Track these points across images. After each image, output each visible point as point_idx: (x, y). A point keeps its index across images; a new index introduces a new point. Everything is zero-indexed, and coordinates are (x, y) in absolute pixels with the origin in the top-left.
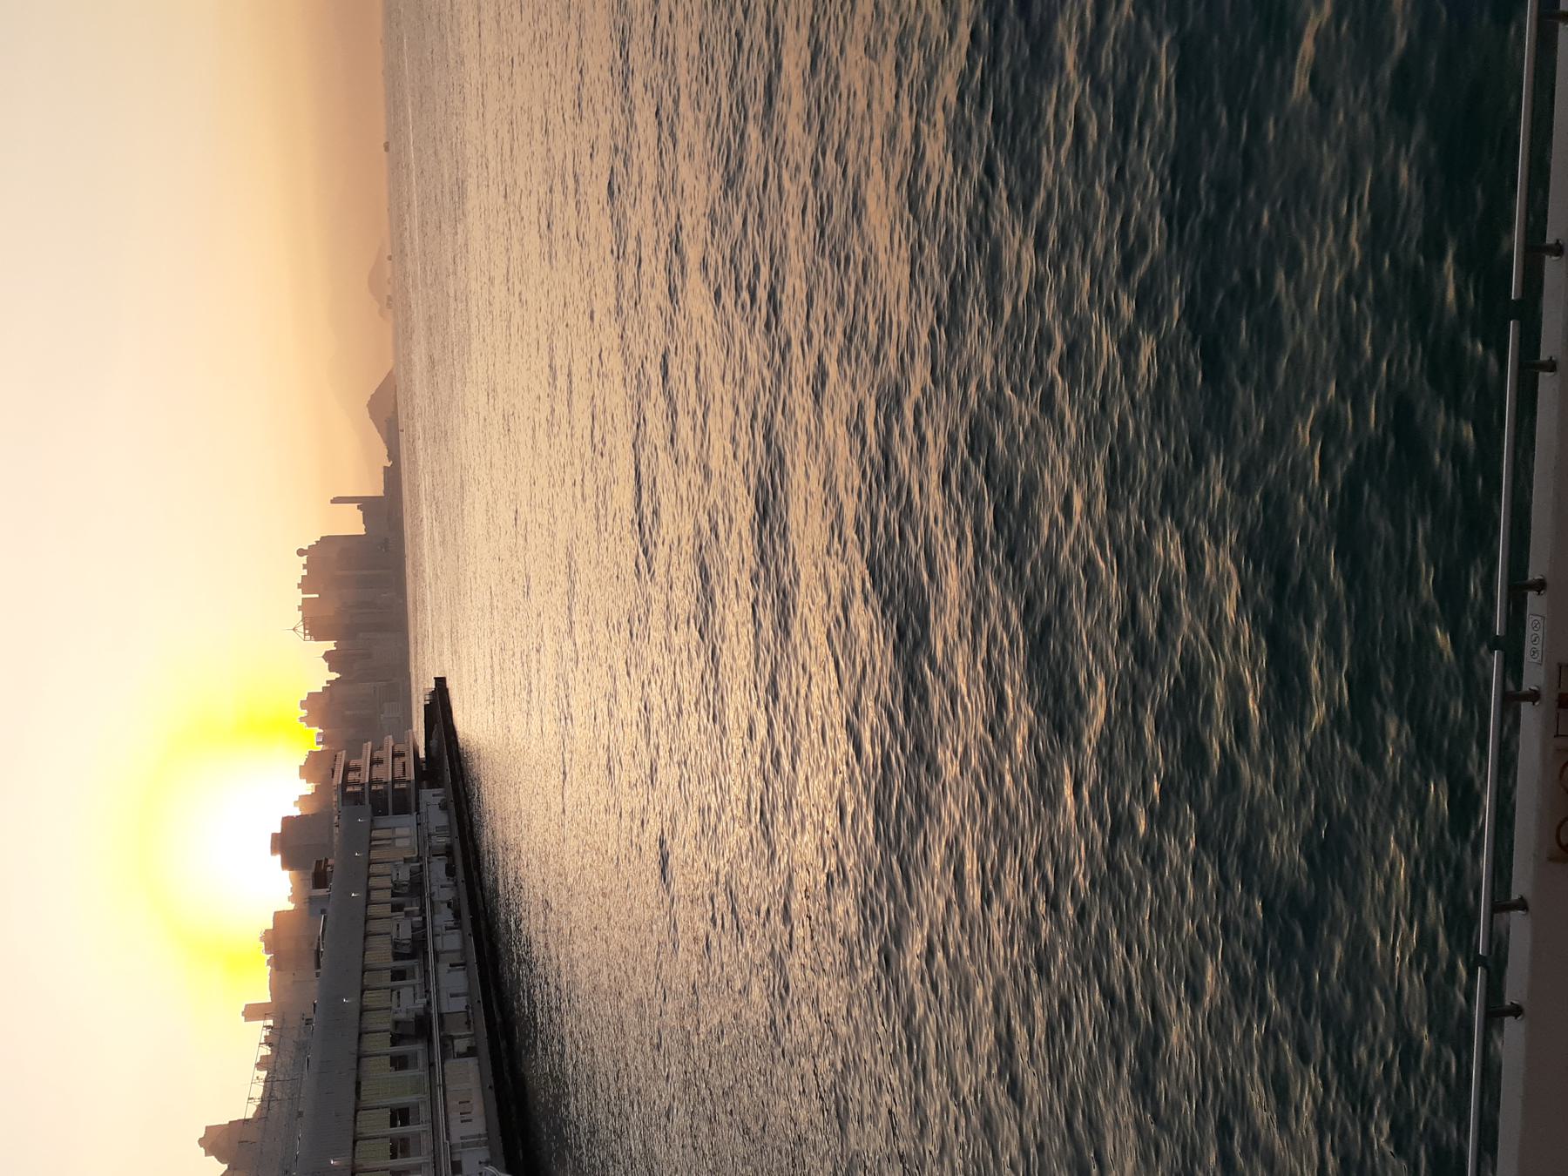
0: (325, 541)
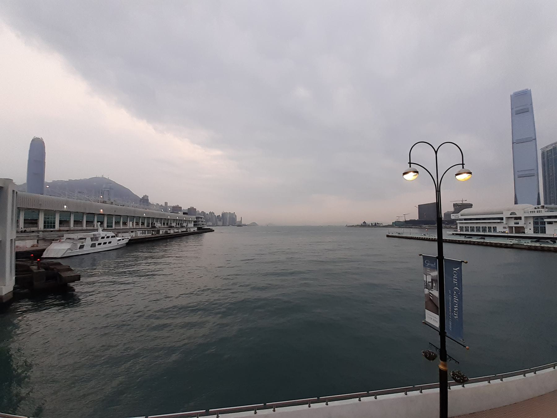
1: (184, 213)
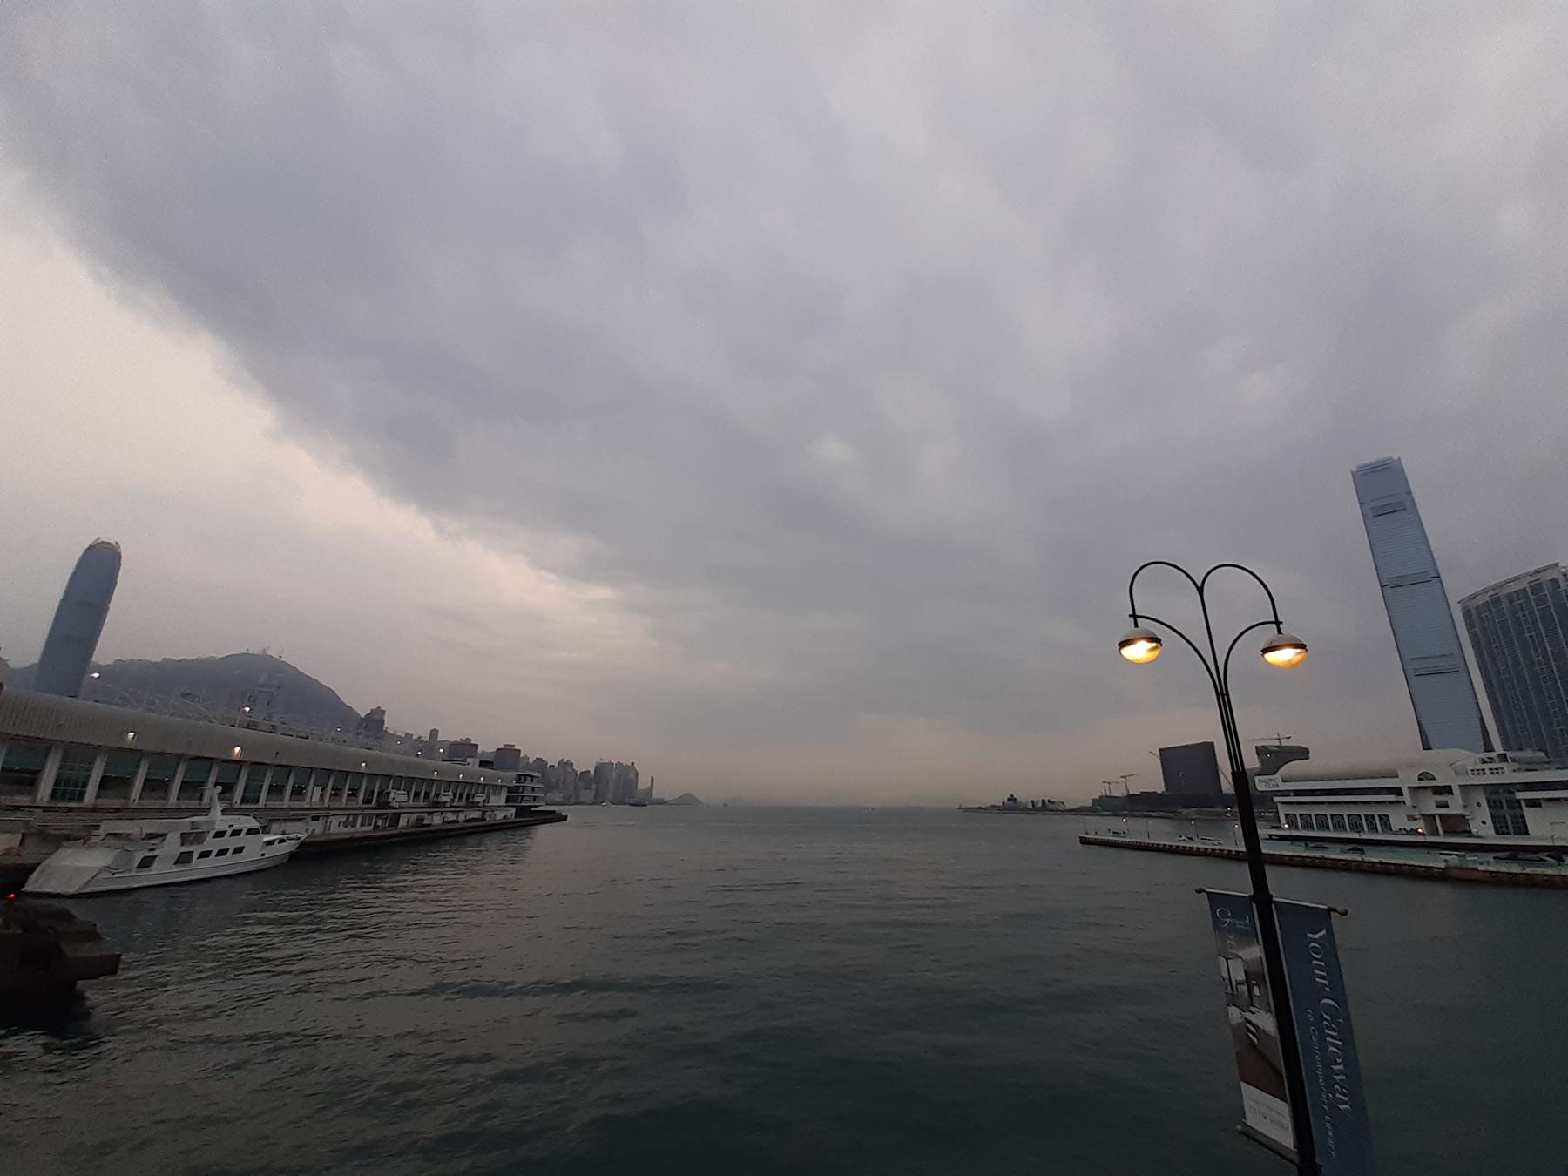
1: (483, 764)
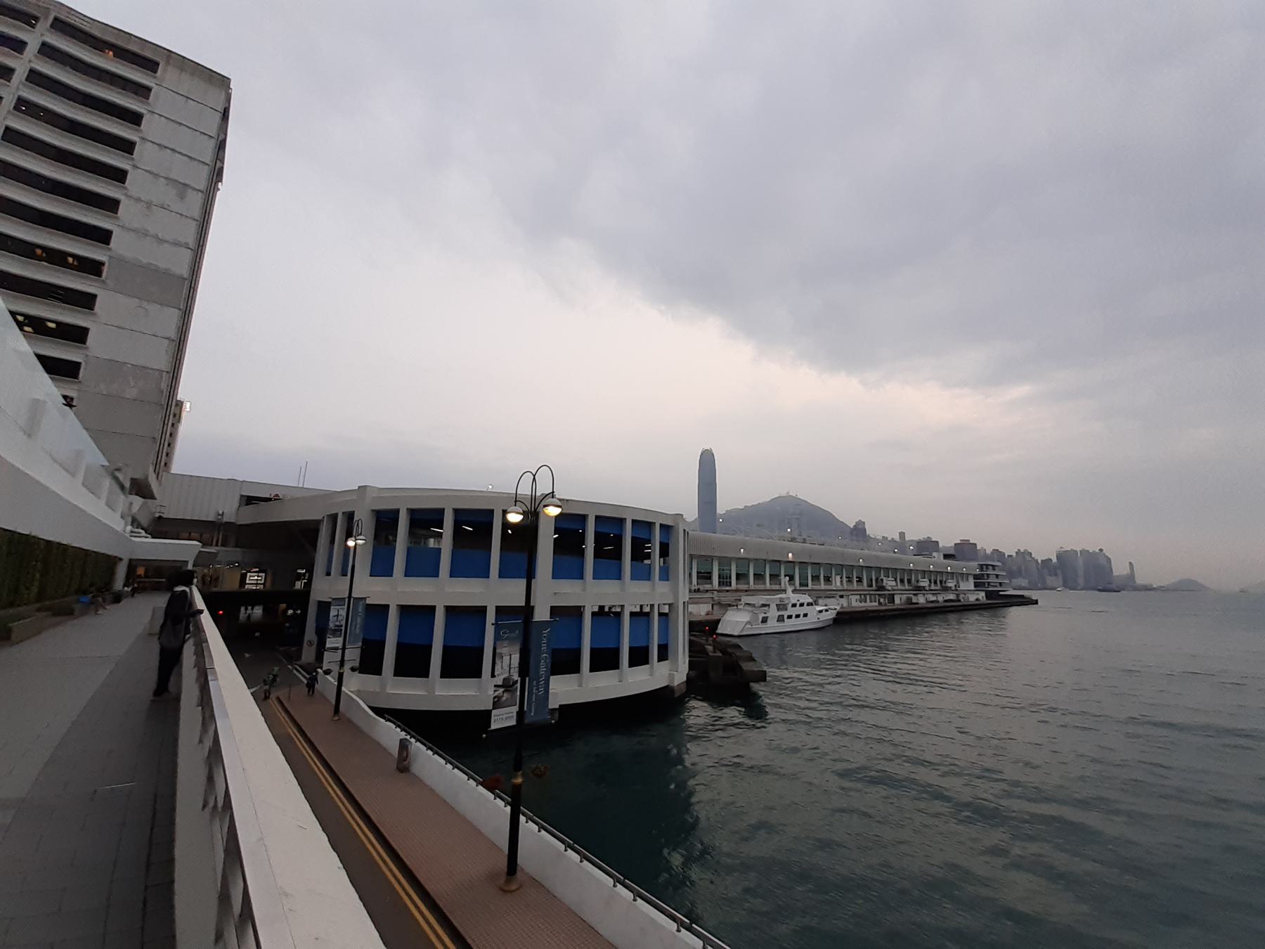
0: (1109, 560)
1: (946, 556)
